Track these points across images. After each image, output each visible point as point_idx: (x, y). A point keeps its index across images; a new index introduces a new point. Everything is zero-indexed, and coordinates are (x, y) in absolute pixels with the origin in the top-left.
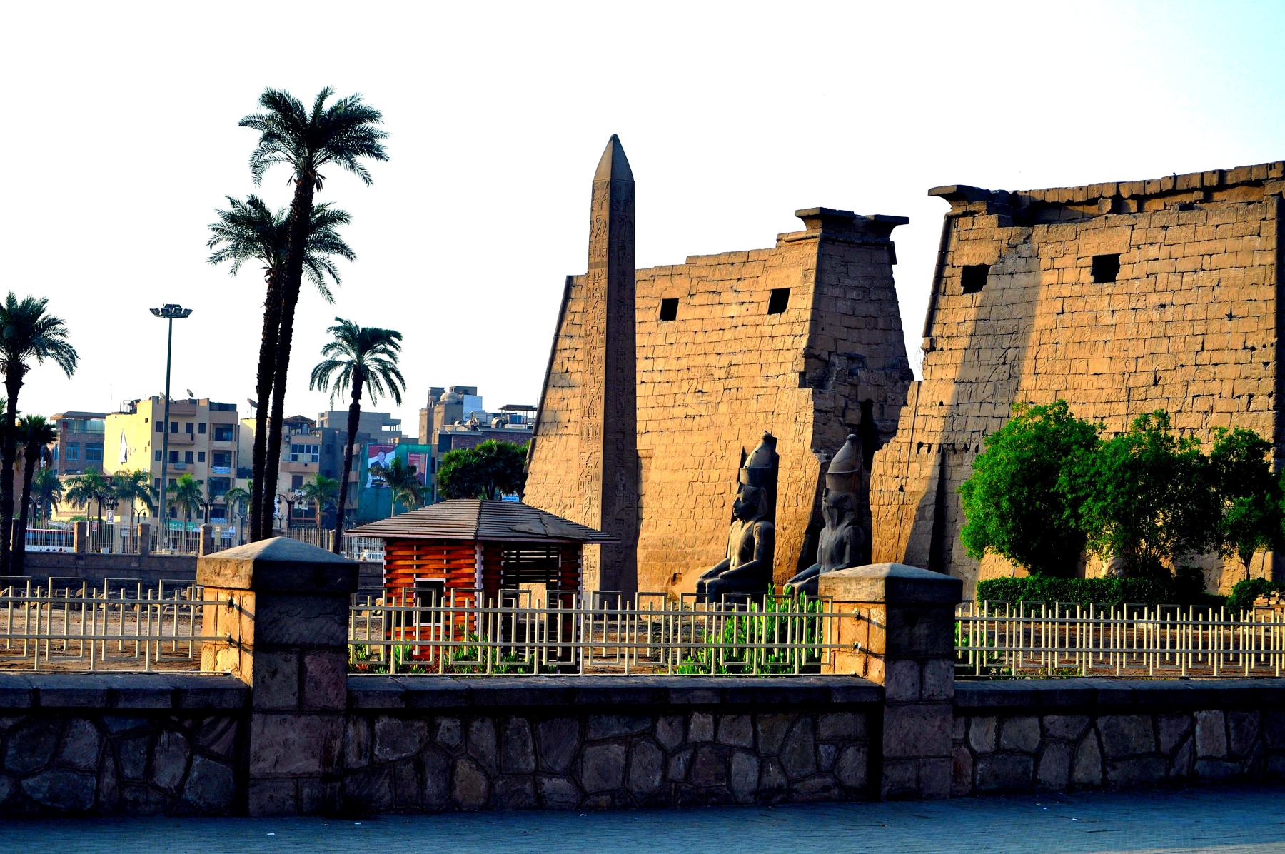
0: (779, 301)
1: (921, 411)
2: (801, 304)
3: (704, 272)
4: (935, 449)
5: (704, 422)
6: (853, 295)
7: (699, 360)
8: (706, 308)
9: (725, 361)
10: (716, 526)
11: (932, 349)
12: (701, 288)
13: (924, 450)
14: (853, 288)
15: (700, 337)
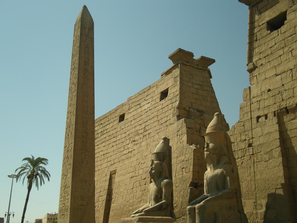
0: (164, 94)
1: (254, 100)
2: (174, 91)
3: (134, 100)
4: (270, 116)
5: (136, 152)
6: (196, 87)
7: (133, 130)
8: (135, 111)
9: (143, 126)
10: (143, 194)
11: (255, 67)
12: (133, 106)
13: (262, 119)
14: (197, 84)
15: (133, 122)
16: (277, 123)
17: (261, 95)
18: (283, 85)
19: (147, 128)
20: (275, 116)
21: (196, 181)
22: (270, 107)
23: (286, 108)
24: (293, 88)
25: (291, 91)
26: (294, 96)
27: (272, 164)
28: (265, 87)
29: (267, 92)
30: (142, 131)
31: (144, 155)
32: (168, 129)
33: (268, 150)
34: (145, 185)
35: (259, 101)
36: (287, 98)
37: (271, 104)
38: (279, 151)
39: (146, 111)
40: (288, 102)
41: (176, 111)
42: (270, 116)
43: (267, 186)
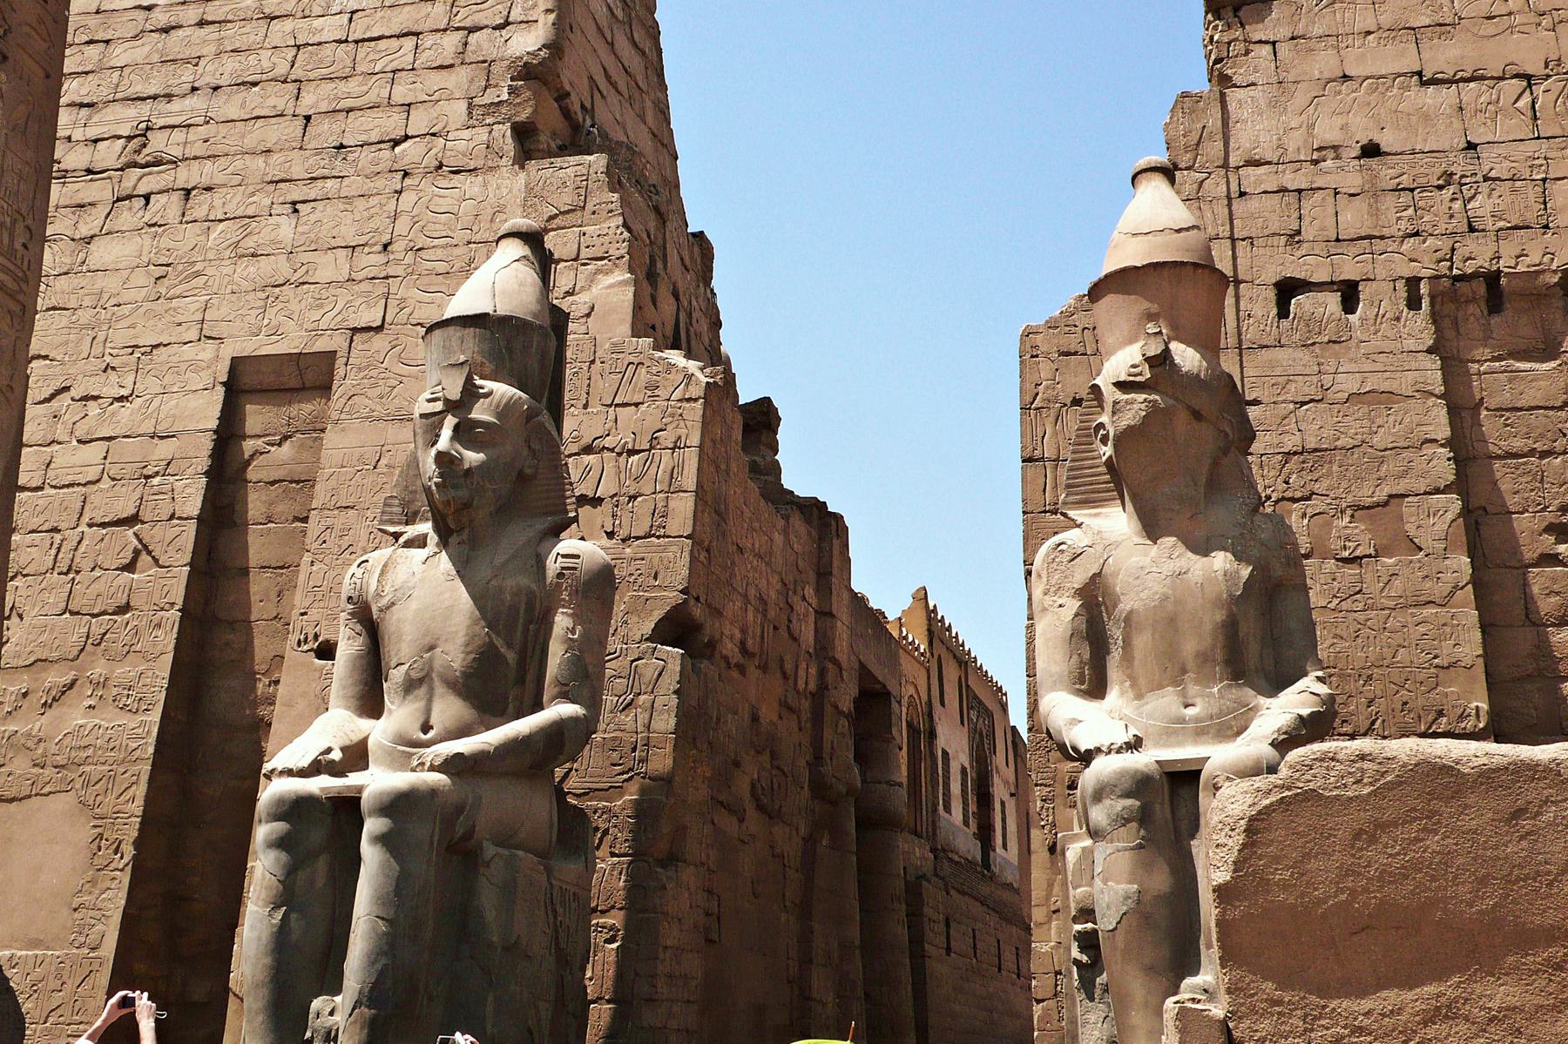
16: (1430, 351)
17: (1315, 162)
18: (1471, 146)
19: (157, 142)
20: (1414, 303)
21: (697, 611)
22: (1379, 245)
23: (1492, 279)
24: (1544, 180)
25: (1532, 193)
26: (1546, 227)
27: (1397, 582)
28: (1339, 121)
29: (1358, 158)
30: (108, 155)
31: (121, 336)
32: (408, 199)
33: (1367, 493)
34: (130, 567)
35: (1300, 191)
36: (1501, 224)
37: (1386, 232)
38: (1450, 516)
39: (160, 18)
40: (1508, 250)
41: (513, 91)
42: (1380, 298)
43: (1362, 708)
